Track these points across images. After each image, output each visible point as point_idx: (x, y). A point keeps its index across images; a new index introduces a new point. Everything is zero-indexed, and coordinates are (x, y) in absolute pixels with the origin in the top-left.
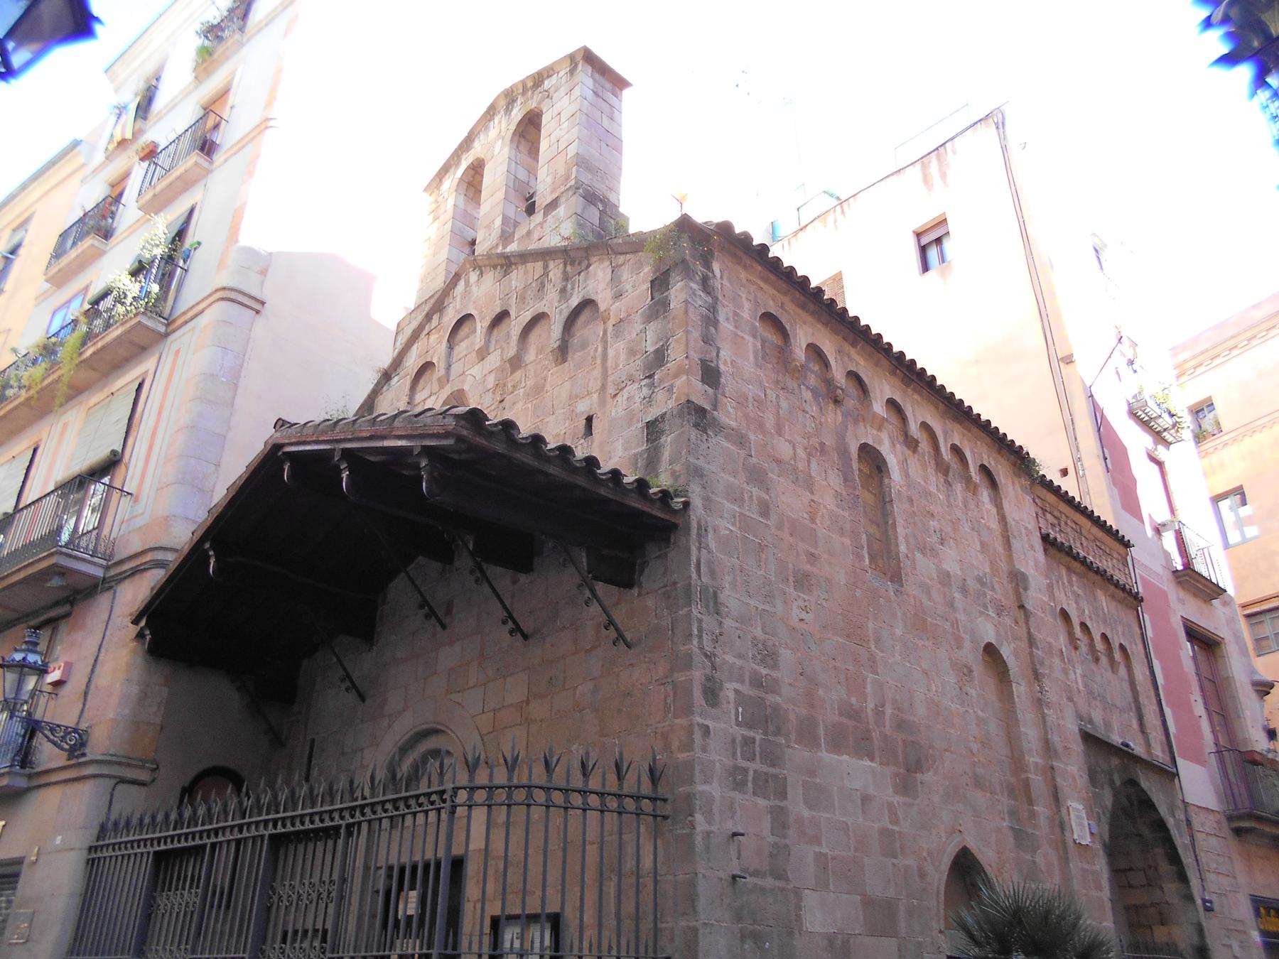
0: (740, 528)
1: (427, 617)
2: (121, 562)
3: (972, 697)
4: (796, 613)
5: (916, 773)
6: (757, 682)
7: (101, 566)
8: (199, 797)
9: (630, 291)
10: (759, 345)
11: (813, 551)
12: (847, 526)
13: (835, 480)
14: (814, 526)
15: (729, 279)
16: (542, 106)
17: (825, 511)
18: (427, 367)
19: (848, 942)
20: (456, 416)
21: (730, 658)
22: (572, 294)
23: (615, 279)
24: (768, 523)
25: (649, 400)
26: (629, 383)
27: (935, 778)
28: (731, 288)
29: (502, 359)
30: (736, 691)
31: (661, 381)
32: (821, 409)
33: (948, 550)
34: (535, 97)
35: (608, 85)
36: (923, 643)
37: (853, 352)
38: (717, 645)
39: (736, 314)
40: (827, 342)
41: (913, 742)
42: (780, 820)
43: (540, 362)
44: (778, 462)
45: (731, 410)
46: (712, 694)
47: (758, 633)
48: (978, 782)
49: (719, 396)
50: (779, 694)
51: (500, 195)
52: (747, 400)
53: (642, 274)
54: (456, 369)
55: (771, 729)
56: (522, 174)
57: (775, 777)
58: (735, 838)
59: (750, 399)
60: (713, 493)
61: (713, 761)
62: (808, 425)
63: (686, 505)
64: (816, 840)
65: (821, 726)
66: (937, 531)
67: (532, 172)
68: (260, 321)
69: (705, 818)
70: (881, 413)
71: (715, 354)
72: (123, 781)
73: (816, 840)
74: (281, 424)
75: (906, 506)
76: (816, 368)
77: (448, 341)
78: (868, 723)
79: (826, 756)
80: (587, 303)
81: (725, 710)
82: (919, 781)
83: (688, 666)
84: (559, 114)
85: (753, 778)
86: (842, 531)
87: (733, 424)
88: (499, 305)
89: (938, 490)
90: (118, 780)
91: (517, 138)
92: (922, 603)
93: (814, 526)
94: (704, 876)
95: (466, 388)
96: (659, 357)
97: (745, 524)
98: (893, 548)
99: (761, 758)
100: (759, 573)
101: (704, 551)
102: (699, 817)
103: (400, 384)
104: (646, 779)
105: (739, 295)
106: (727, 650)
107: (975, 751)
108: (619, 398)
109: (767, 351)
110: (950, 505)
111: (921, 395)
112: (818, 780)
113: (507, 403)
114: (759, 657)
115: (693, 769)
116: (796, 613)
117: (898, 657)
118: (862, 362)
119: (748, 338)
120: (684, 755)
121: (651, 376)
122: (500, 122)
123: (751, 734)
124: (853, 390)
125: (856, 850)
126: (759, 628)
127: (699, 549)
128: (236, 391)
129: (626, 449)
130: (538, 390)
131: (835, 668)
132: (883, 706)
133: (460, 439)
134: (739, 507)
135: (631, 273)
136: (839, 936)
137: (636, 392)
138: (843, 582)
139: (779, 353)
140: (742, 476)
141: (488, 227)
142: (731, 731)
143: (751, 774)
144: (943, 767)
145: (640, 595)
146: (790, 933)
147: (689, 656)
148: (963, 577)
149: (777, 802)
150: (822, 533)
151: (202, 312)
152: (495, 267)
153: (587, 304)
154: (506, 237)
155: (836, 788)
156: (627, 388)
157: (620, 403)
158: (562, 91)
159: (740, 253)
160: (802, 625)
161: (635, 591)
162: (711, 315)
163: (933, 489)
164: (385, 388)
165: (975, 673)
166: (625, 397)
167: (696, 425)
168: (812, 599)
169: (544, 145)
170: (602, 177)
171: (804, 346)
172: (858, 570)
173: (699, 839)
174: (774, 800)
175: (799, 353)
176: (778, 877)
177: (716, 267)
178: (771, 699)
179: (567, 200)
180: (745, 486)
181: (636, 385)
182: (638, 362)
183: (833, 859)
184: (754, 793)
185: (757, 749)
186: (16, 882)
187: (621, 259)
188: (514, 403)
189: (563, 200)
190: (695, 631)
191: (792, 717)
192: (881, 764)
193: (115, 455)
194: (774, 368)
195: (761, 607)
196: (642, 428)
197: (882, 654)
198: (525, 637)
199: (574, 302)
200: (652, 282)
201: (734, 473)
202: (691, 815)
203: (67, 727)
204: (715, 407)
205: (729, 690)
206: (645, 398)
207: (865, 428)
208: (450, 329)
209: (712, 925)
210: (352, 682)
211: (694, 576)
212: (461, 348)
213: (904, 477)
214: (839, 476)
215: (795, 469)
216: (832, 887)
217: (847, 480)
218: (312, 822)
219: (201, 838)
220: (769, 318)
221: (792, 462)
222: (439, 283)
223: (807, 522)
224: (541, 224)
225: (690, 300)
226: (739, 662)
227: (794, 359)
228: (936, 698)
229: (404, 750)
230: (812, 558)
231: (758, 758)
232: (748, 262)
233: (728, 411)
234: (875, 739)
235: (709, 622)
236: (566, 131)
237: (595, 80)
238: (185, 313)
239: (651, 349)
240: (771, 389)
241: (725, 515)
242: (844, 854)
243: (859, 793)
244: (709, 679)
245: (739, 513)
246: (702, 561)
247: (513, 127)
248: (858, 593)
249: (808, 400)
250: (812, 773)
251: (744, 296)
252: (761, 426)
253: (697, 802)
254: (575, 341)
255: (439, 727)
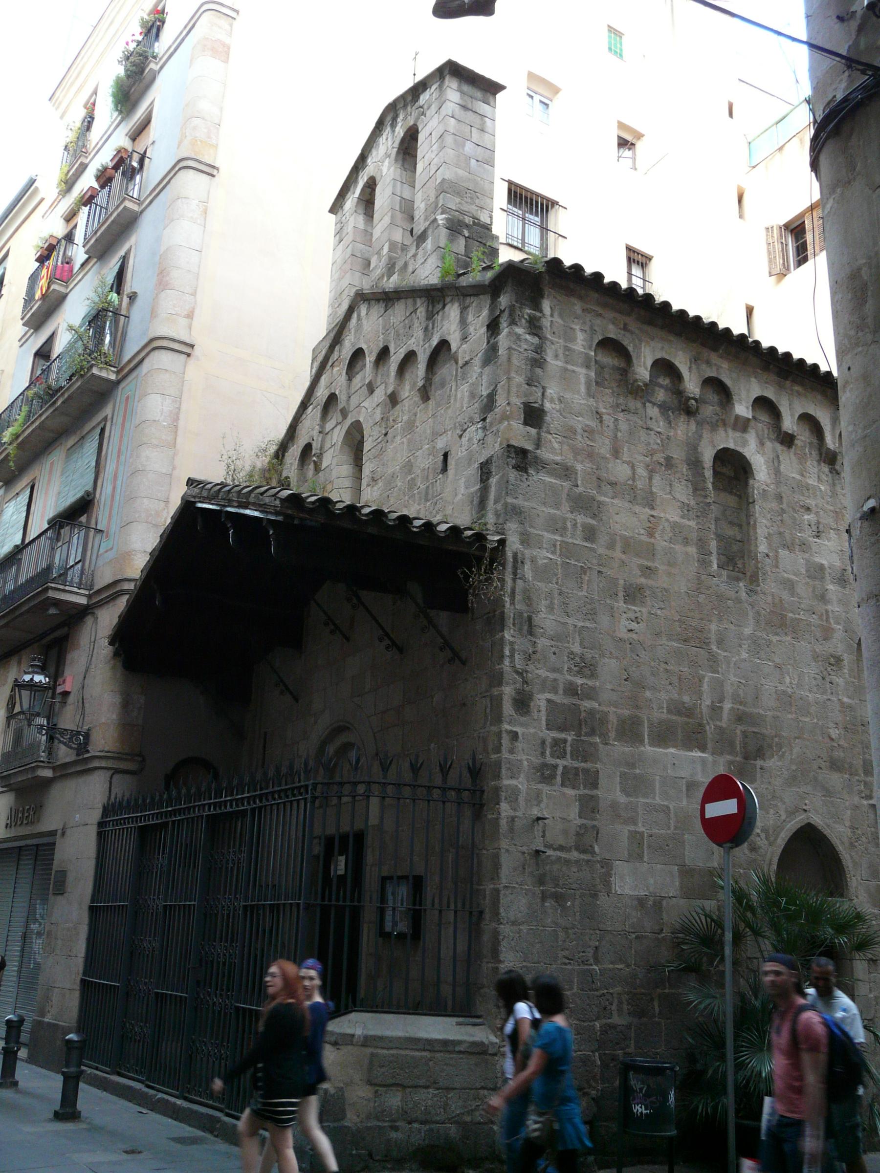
0: (560, 555)
1: (332, 632)
2: (99, 592)
3: (837, 685)
4: (624, 624)
5: (755, 760)
6: (572, 690)
7: (84, 595)
8: (181, 782)
9: (473, 334)
10: (593, 374)
11: (649, 564)
12: (694, 536)
13: (683, 492)
14: (652, 540)
15: (561, 315)
16: (418, 124)
17: (666, 524)
18: (332, 399)
19: (660, 903)
20: (281, 499)
21: (543, 673)
22: (432, 334)
23: (463, 322)
24: (594, 546)
25: (482, 441)
26: (470, 425)
27: (779, 763)
28: (562, 322)
29: (386, 394)
30: (549, 701)
31: (491, 424)
32: (670, 422)
33: (826, 543)
34: (413, 113)
35: (479, 94)
36: (778, 638)
37: (714, 357)
38: (529, 663)
39: (567, 349)
40: (680, 353)
41: (754, 732)
42: (589, 806)
43: (412, 398)
44: (612, 484)
45: (556, 446)
46: (523, 703)
47: (577, 648)
48: (835, 765)
49: (543, 434)
50: (596, 700)
51: (387, 220)
52: (575, 432)
53: (481, 318)
54: (354, 401)
55: (584, 730)
56: (407, 195)
57: (586, 771)
58: (540, 822)
59: (579, 431)
60: (531, 526)
61: (520, 761)
62: (652, 441)
63: (502, 542)
64: (633, 821)
65: (646, 725)
66: (813, 524)
67: (414, 195)
68: (191, 361)
69: (511, 806)
70: (746, 415)
71: (540, 394)
72: (117, 771)
73: (633, 821)
74: (191, 482)
75: (774, 505)
76: (665, 381)
77: (347, 373)
78: (702, 718)
79: (648, 749)
80: (444, 344)
81: (536, 718)
82: (758, 767)
83: (500, 683)
84: (431, 134)
85: (562, 773)
86: (686, 541)
87: (558, 458)
88: (382, 341)
89: (819, 479)
90: (113, 771)
91: (401, 156)
92: (781, 600)
93: (652, 540)
94: (507, 851)
95: (361, 420)
96: (489, 403)
97: (567, 550)
98: (753, 548)
99: (572, 756)
100: (580, 594)
101: (519, 582)
102: (504, 806)
103: (313, 413)
104: (466, 774)
105: (571, 328)
106: (539, 666)
107: (833, 737)
108: (463, 439)
109: (607, 376)
110: (834, 494)
111: (802, 384)
112: (638, 771)
113: (390, 435)
114: (576, 669)
115: (500, 768)
116: (624, 624)
117: (744, 655)
118: (725, 365)
119: (582, 371)
120: (496, 756)
121: (484, 420)
122: (387, 139)
123: (562, 736)
124: (712, 396)
125: (676, 828)
126: (577, 644)
127: (514, 580)
128: (176, 432)
129: (466, 488)
130: (410, 426)
131: (667, 671)
132: (721, 701)
133: (286, 516)
134: (561, 536)
135: (474, 315)
136: (651, 898)
137: (474, 432)
138: (684, 589)
139: (621, 375)
140: (566, 507)
141: (378, 253)
142: (541, 734)
143: (560, 769)
144: (791, 754)
145: (472, 619)
146: (595, 896)
147: (502, 673)
148: (844, 567)
149: (586, 791)
150: (661, 542)
151: (141, 361)
152: (378, 300)
153: (444, 344)
154: (390, 269)
155: (658, 778)
156: (469, 430)
157: (463, 444)
158: (434, 108)
159: (572, 286)
160: (630, 635)
161: (470, 615)
162: (538, 357)
163: (812, 481)
164: (304, 416)
165: (846, 662)
166: (467, 439)
167: (516, 467)
168: (644, 610)
169: (420, 167)
170: (471, 198)
171: (649, 363)
172: (703, 577)
173: (503, 822)
174: (585, 788)
175: (643, 371)
176: (584, 852)
177: (546, 305)
178: (587, 704)
179: (433, 232)
180: (569, 515)
181: (473, 428)
182: (476, 405)
183: (651, 836)
184: (563, 785)
185: (569, 749)
186: (54, 849)
187: (468, 300)
188: (394, 437)
189: (430, 232)
190: (507, 652)
191: (612, 718)
192: (713, 754)
193: (88, 496)
194: (613, 392)
195: (580, 624)
196: (478, 468)
197: (725, 654)
198: (401, 650)
199: (435, 342)
200: (488, 326)
201: (557, 506)
202: (498, 804)
203: (72, 731)
204: (538, 446)
205: (541, 700)
206: (479, 441)
207: (726, 431)
208: (347, 361)
209: (514, 887)
210: (286, 686)
211: (507, 605)
212: (357, 380)
213: (773, 476)
214: (687, 487)
215: (633, 488)
216: (646, 859)
217: (697, 488)
218: (231, 806)
219: (166, 817)
220: (608, 344)
221: (630, 482)
222: (345, 306)
223: (644, 538)
224: (415, 256)
225: (514, 346)
226: (552, 676)
227: (636, 380)
228: (789, 690)
229: (324, 744)
230: (648, 571)
231: (568, 756)
232: (583, 292)
233: (554, 448)
234: (708, 733)
235: (522, 643)
236: (436, 152)
237: (462, 92)
238: (130, 361)
239: (485, 393)
240: (609, 414)
241: (545, 546)
242: (662, 831)
243: (685, 780)
244: (519, 692)
245: (562, 541)
246: (517, 590)
247: (396, 145)
248: (702, 598)
249: (654, 417)
250: (633, 766)
251: (577, 327)
252: (591, 455)
253: (503, 794)
254: (437, 379)
255: (348, 725)
